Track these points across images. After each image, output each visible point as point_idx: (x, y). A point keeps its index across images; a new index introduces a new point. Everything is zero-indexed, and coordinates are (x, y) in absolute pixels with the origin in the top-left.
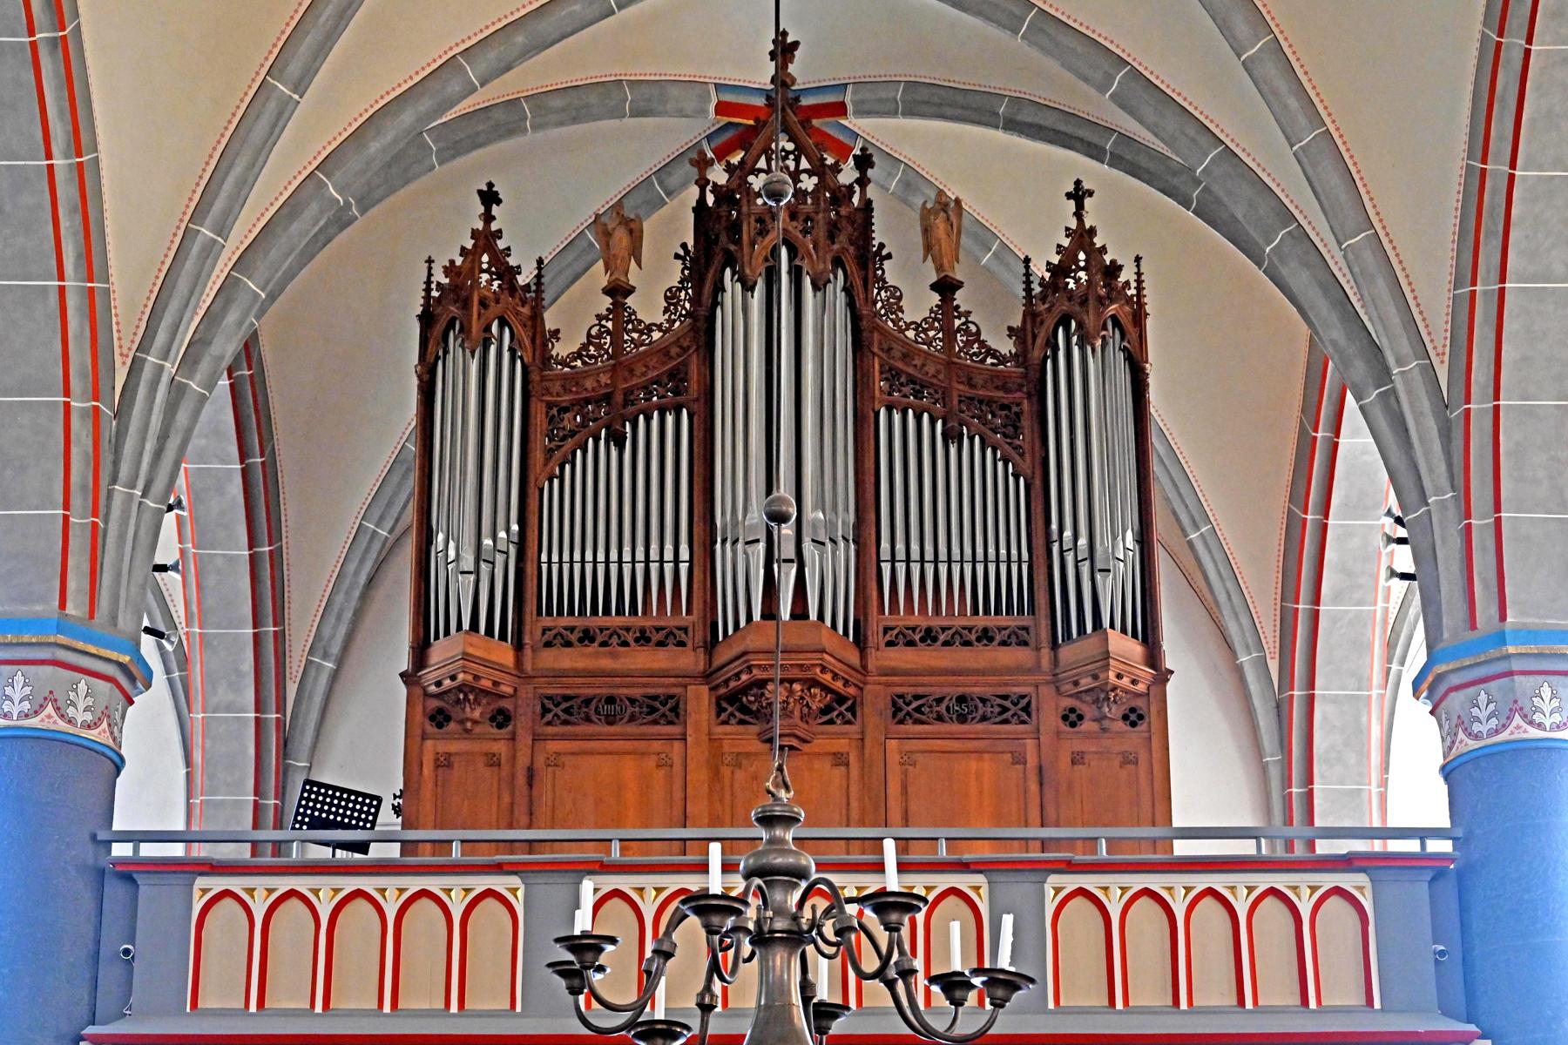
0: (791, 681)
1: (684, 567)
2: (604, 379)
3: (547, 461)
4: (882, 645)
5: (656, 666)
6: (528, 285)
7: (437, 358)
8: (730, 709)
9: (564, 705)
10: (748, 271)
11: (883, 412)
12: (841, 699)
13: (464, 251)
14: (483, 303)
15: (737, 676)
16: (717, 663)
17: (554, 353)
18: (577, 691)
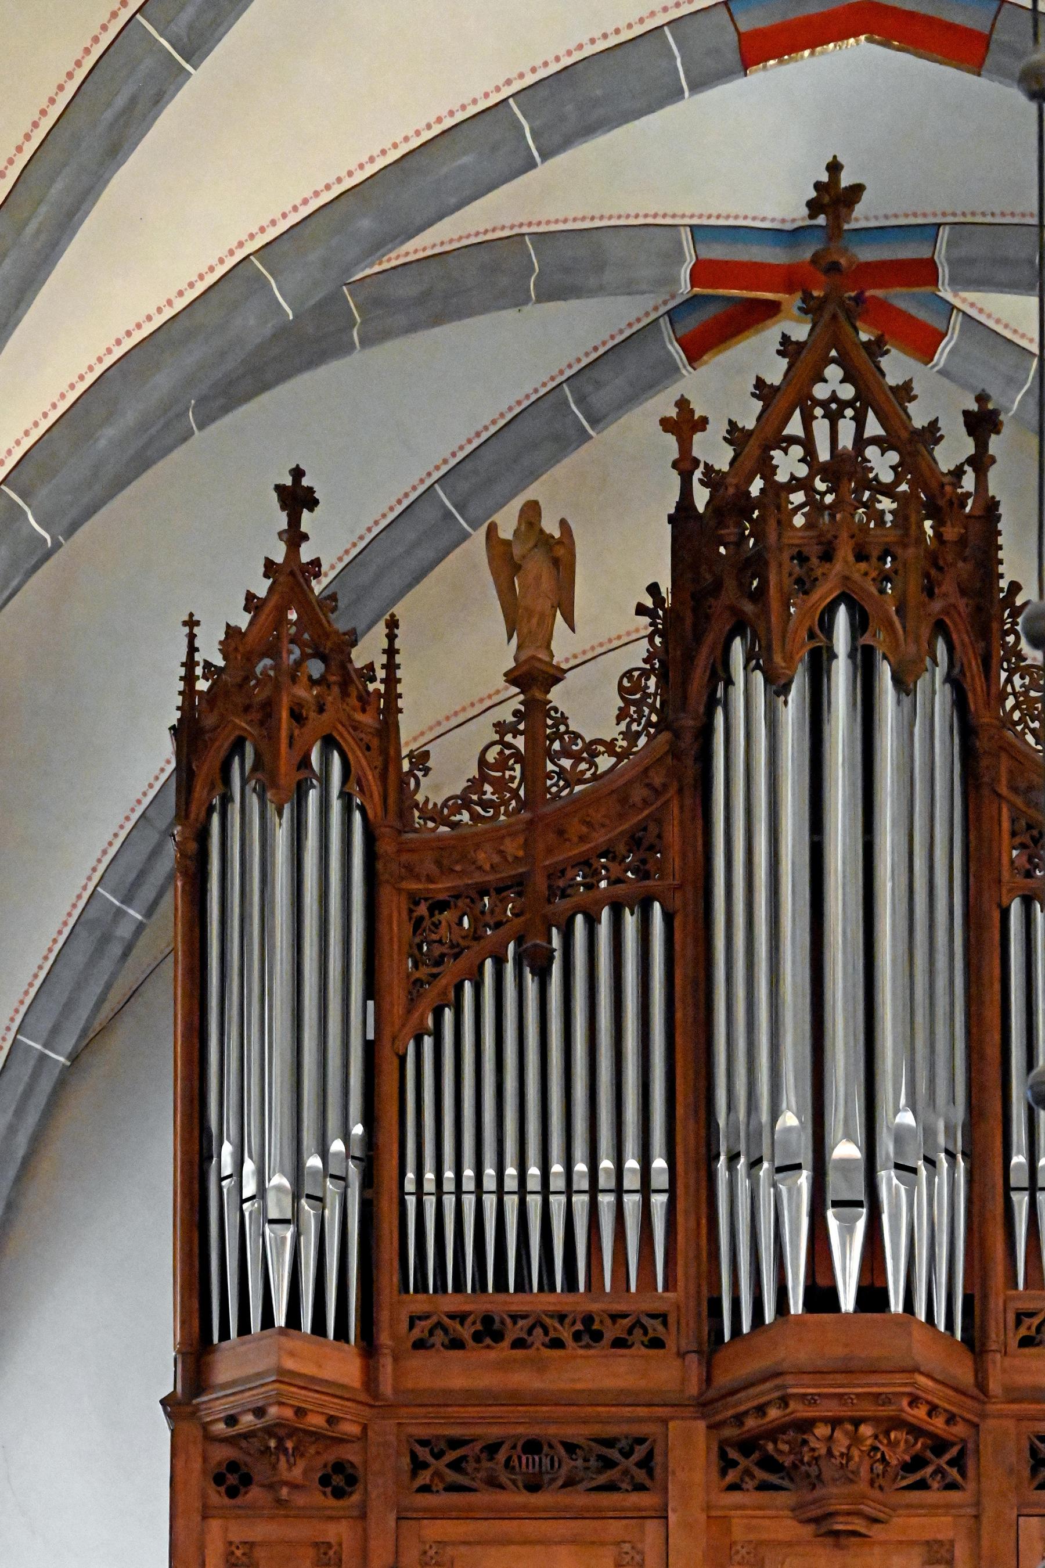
0: (857, 1422)
1: (659, 1201)
2: (512, 847)
3: (412, 1002)
4: (1013, 1343)
5: (609, 1383)
6: (371, 667)
7: (211, 809)
8: (744, 1462)
9: (451, 1456)
10: (778, 659)
11: (1016, 909)
12: (940, 1446)
13: (251, 602)
14: (297, 716)
15: (761, 1410)
16: (723, 1380)
17: (420, 798)
18: (478, 1431)
